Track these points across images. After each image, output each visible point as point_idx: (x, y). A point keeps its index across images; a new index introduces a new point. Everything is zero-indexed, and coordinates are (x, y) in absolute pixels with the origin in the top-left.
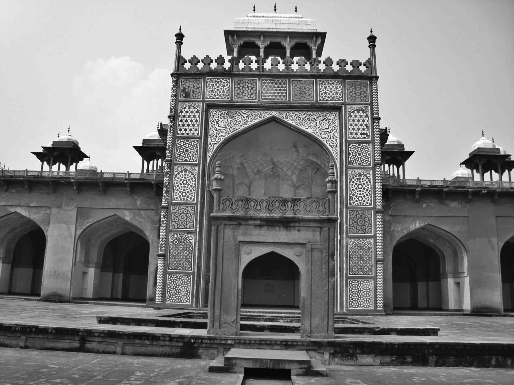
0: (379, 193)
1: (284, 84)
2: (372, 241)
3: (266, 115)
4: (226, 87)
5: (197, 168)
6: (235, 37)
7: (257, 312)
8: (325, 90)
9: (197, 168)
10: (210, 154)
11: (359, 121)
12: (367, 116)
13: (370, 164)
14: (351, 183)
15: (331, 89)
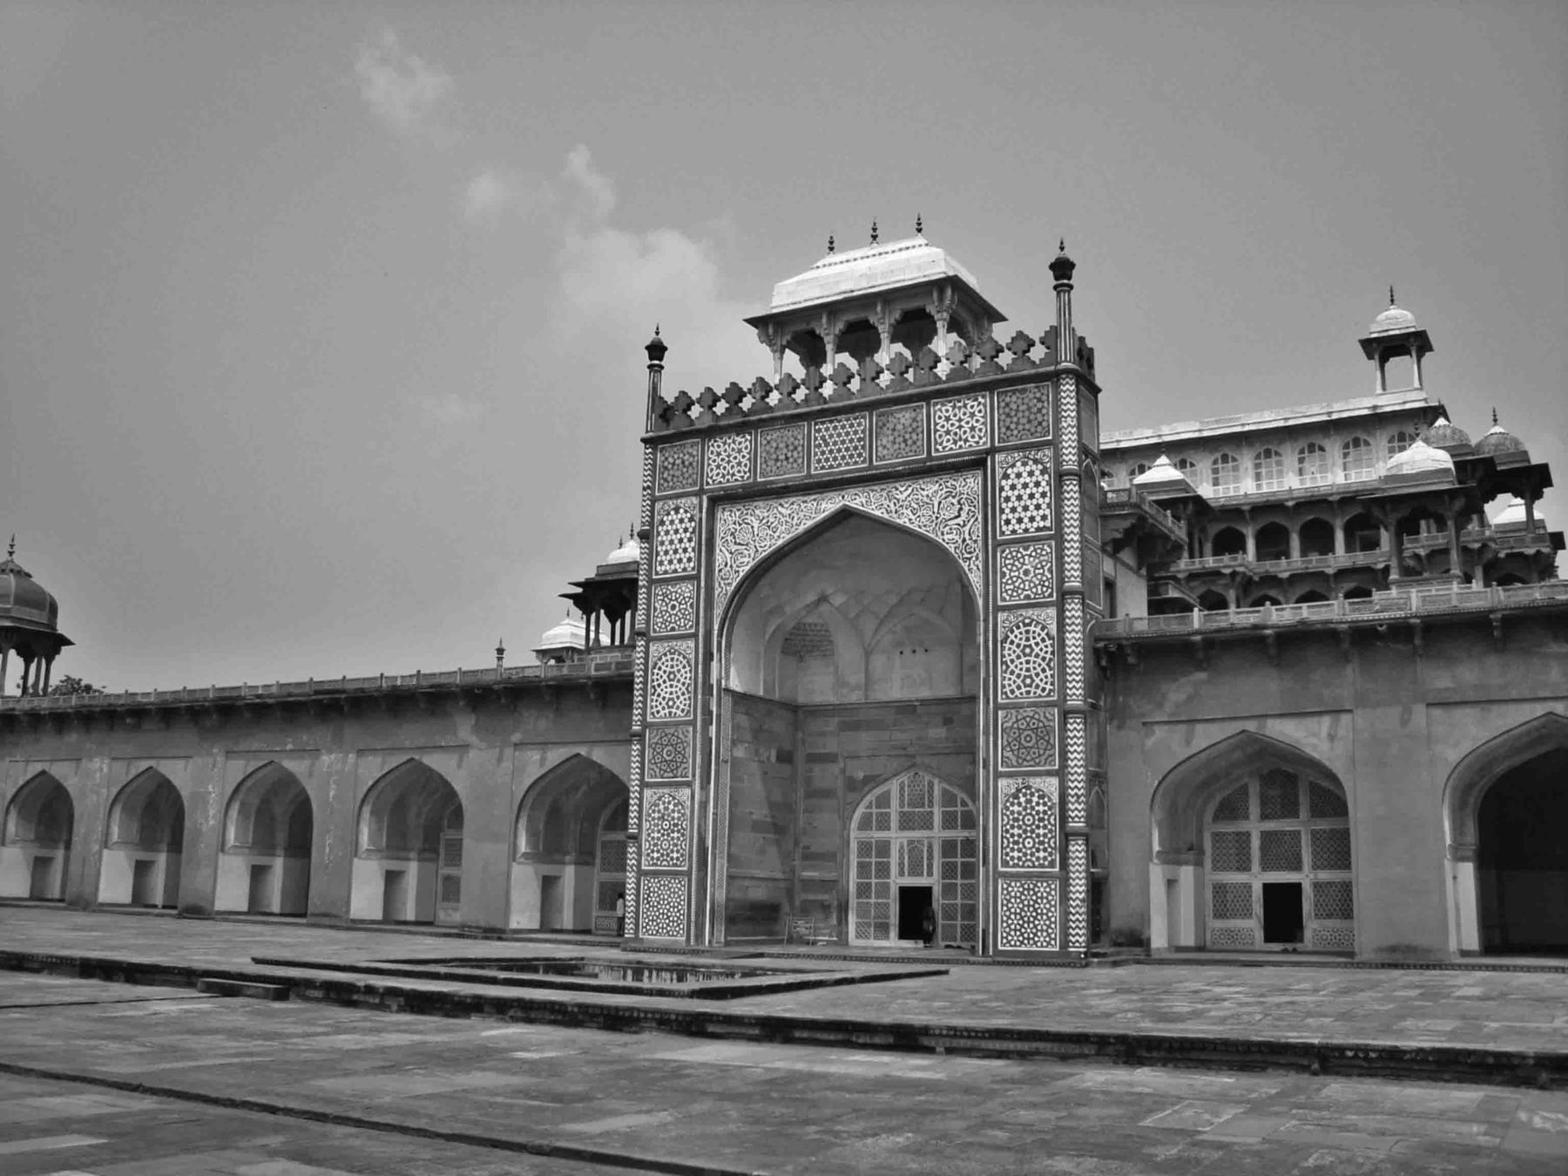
0: (1076, 661)
1: (859, 424)
2: (1055, 781)
3: (829, 505)
4: (745, 452)
5: (691, 644)
6: (771, 331)
7: (761, 955)
8: (948, 426)
9: (691, 644)
10: (718, 612)
11: (1025, 486)
12: (1042, 473)
13: (1051, 595)
14: (1007, 646)
15: (960, 420)
